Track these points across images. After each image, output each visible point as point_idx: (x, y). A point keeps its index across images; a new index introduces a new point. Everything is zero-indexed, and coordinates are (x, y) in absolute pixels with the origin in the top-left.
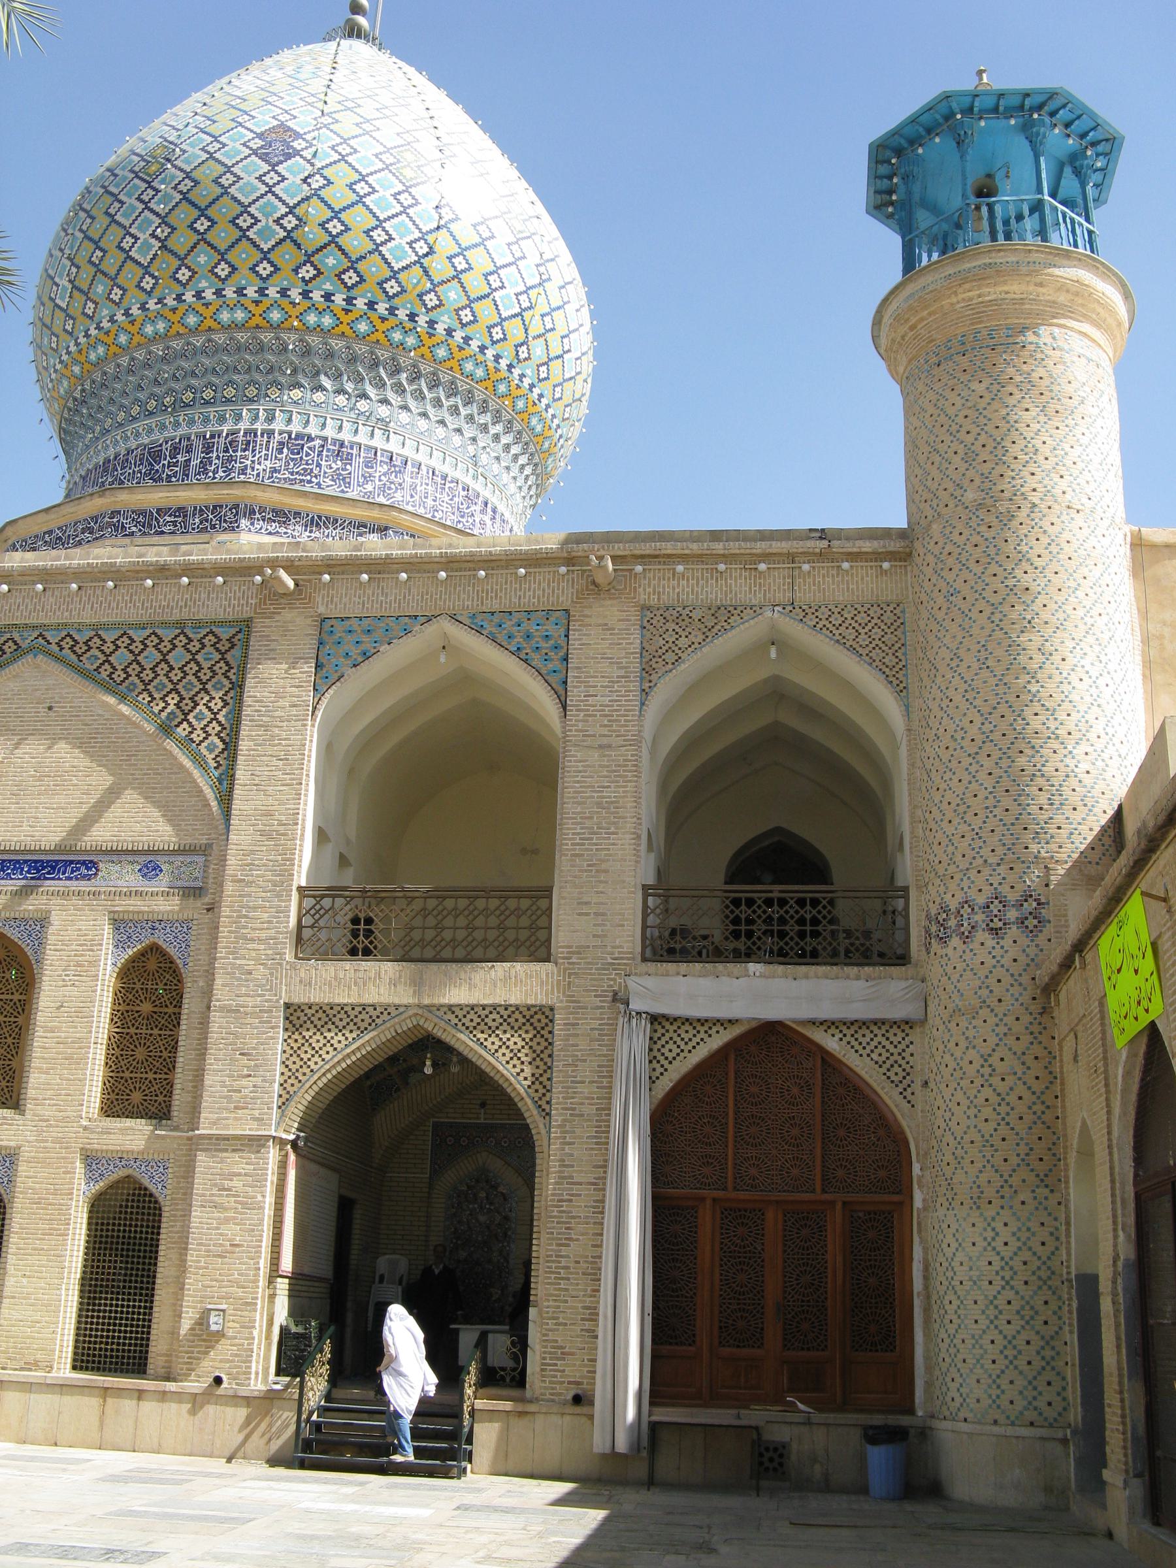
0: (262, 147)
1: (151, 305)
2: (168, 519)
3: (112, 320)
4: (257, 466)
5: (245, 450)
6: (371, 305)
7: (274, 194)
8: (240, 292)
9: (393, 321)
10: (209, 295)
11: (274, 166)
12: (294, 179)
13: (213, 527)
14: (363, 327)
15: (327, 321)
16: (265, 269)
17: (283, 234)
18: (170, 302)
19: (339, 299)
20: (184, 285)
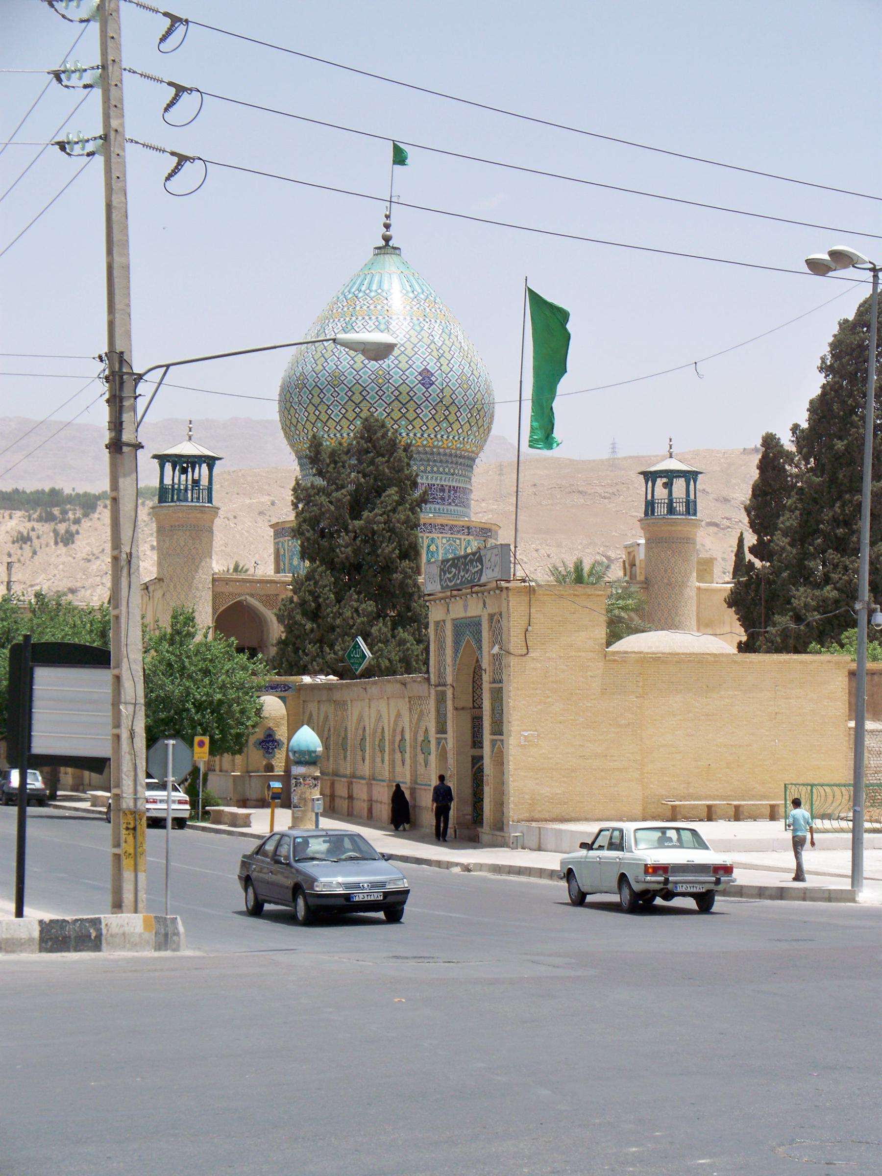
8: (415, 435)
11: (427, 389)
12: (434, 395)
14: (450, 444)
15: (440, 443)
16: (424, 428)
19: (445, 437)
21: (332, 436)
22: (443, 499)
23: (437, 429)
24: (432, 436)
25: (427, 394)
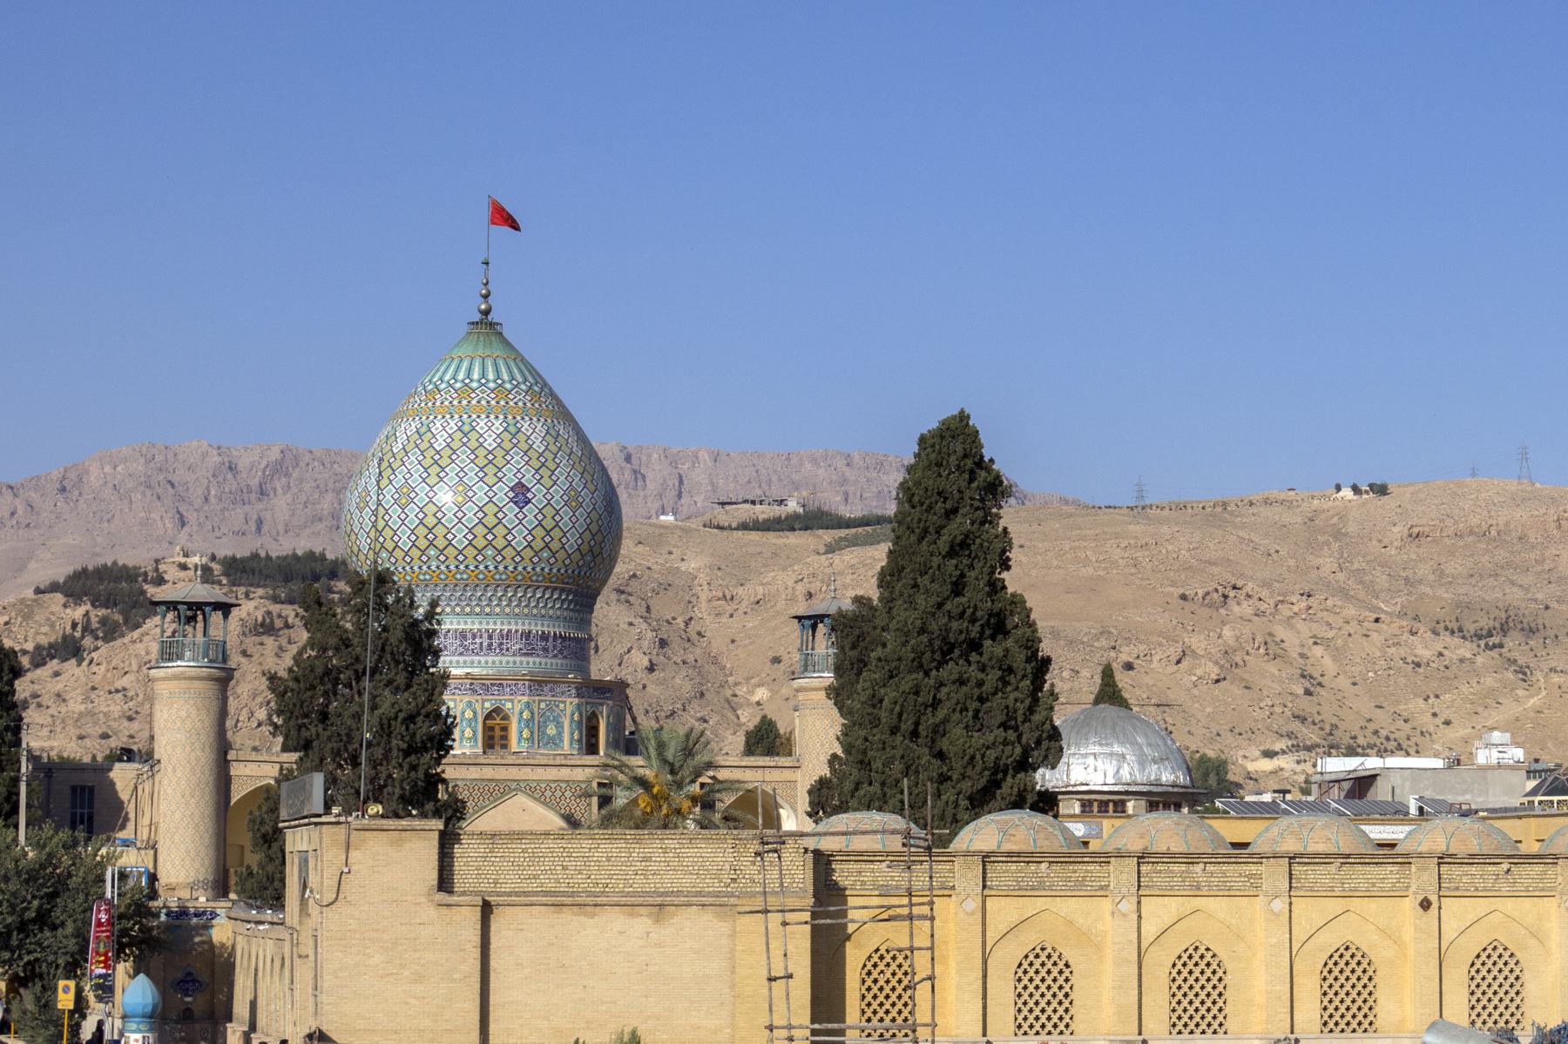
1: (462, 567)
16: (518, 559)
22: (545, 649)
25: (521, 516)
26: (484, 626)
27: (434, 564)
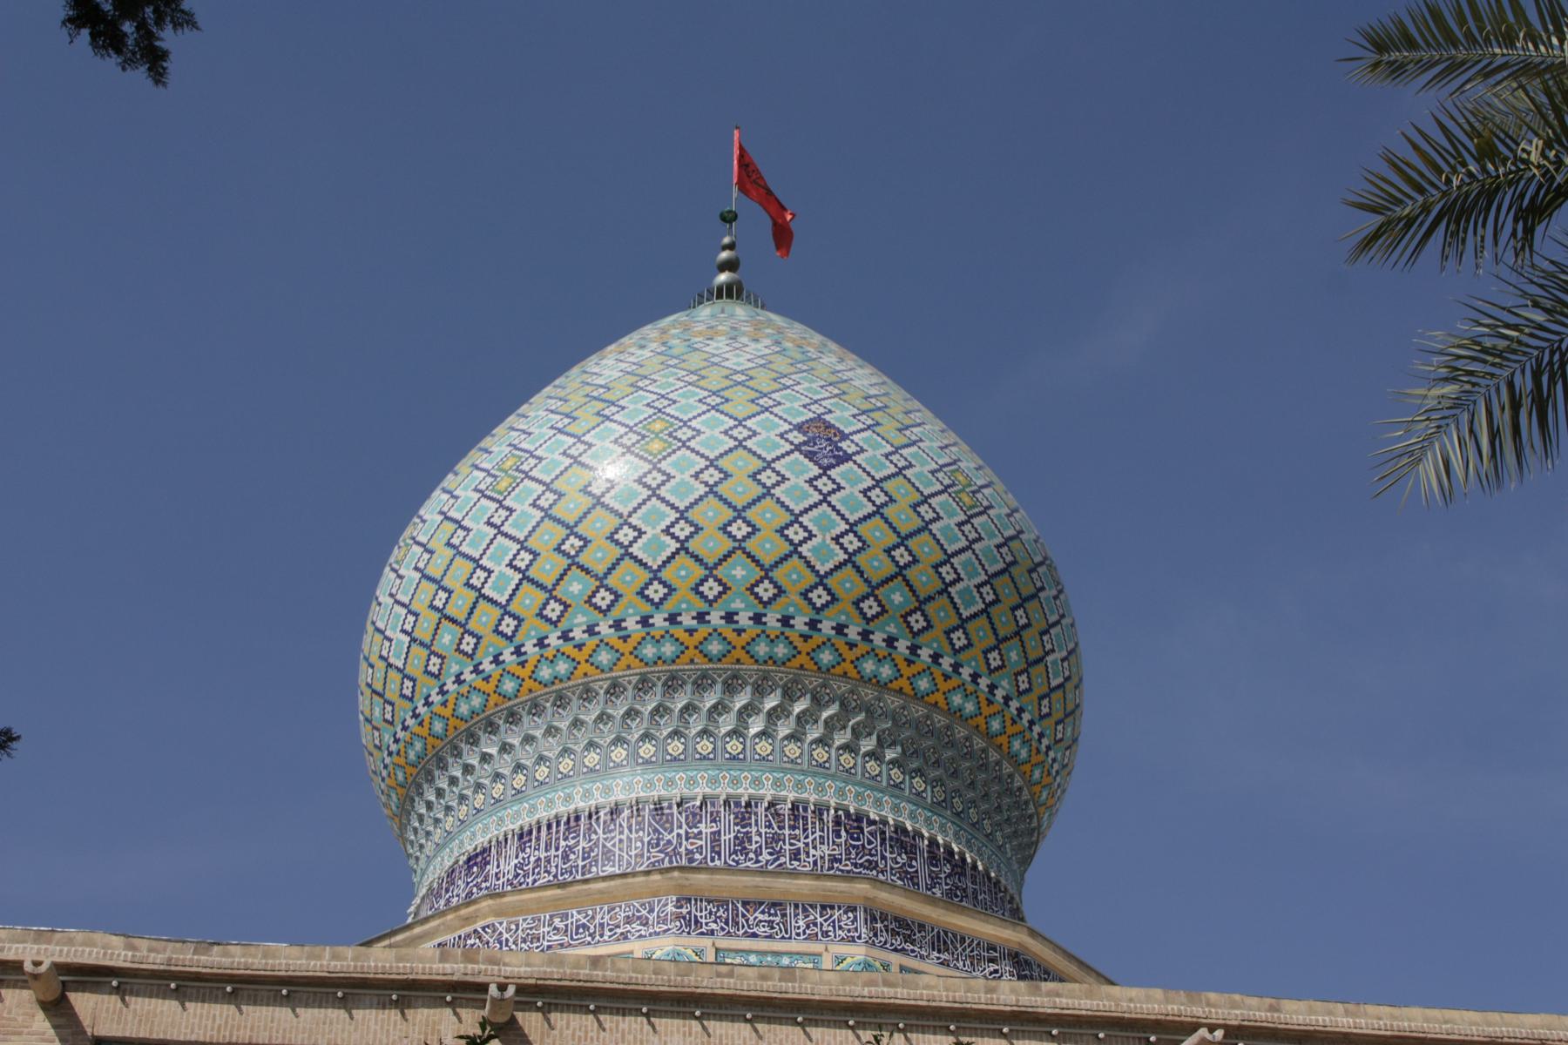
0: (805, 443)
1: (659, 620)
2: (761, 917)
3: (591, 630)
4: (812, 852)
5: (793, 828)
6: (936, 657)
7: (829, 504)
9: (955, 681)
10: (743, 619)
11: (825, 469)
12: (852, 491)
13: (826, 934)
14: (923, 684)
17: (842, 556)
18: (687, 620)
19: (902, 645)
20: (711, 603)
21: (487, 666)
23: (871, 608)
24: (853, 633)
26: (723, 790)
27: (579, 621)
